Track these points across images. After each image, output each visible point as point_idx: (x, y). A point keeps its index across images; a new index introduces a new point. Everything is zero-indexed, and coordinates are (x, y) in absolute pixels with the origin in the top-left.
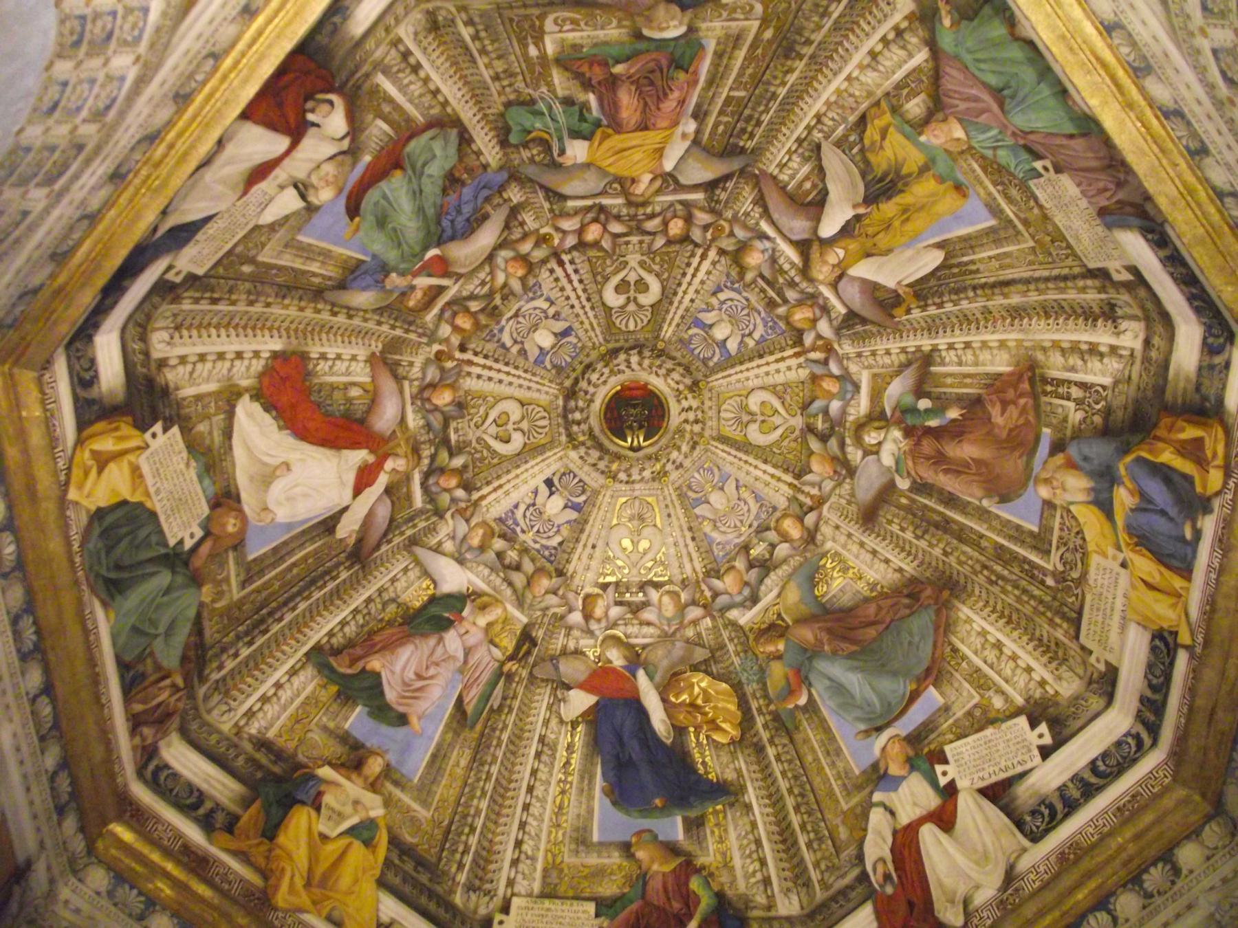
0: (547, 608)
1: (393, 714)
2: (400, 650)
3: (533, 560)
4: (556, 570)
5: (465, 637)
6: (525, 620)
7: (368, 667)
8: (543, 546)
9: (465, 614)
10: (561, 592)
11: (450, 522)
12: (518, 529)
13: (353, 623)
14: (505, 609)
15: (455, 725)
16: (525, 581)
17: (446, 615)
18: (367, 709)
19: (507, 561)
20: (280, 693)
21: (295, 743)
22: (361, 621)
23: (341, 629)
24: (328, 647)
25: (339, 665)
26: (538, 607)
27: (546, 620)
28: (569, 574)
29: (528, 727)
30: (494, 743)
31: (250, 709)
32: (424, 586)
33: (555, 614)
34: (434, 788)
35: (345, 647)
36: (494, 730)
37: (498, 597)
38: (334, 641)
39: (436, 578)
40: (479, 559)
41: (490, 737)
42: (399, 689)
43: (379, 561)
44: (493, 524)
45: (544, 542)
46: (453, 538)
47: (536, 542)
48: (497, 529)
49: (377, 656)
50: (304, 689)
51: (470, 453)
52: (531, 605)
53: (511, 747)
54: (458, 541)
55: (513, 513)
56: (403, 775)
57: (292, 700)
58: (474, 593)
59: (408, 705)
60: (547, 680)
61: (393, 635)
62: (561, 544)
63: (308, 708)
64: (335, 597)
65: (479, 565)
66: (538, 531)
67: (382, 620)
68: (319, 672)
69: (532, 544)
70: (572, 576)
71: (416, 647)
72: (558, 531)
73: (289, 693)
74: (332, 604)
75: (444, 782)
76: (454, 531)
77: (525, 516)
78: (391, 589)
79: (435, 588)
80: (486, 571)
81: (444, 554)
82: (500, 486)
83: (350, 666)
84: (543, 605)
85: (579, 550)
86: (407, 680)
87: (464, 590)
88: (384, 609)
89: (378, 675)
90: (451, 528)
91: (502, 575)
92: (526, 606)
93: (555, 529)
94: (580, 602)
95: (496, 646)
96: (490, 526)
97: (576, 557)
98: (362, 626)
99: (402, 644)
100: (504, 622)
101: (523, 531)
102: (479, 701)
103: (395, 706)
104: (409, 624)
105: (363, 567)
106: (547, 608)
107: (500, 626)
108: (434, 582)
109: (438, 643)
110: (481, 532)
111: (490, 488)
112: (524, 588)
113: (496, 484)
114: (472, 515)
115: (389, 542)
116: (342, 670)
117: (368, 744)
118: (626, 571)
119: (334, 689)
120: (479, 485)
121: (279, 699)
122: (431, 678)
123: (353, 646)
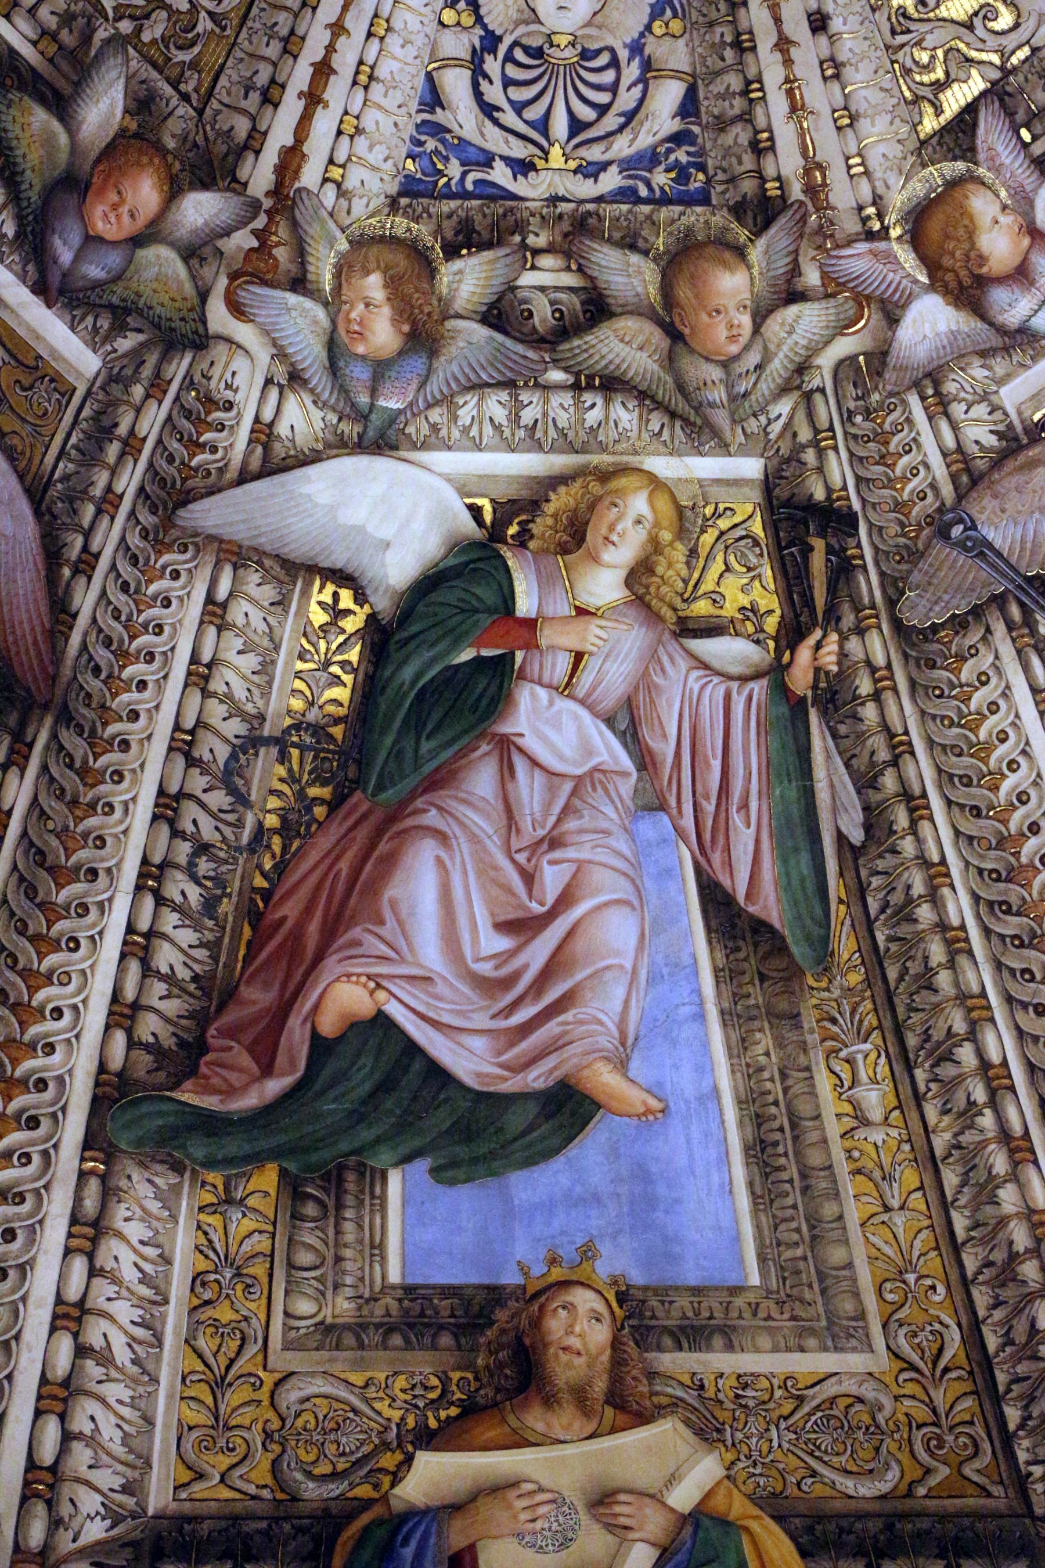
0: (802, 369)
1: (532, 1109)
2: (391, 892)
3: (630, 243)
4: (738, 211)
5: (585, 680)
6: (752, 467)
7: (328, 1025)
8: (627, 165)
9: (525, 605)
10: (812, 277)
11: (244, 332)
12: (500, 175)
13: (170, 920)
14: (655, 483)
15: (757, 996)
16: (657, 337)
17: (466, 655)
18: (421, 1166)
19: (543, 314)
20: (94, 1333)
21: (262, 1461)
22: (194, 894)
23: (148, 970)
24: (144, 1060)
25: (230, 1092)
26: (765, 387)
27: (825, 410)
28: (796, 192)
29: (1017, 820)
30: (937, 952)
31: (32, 1465)
32: (319, 617)
33: (845, 365)
34: (837, 1255)
35: (201, 1019)
36: (905, 913)
37: (596, 459)
38: (149, 1026)
39: (338, 559)
40: (436, 386)
41: (910, 945)
42: (481, 1020)
43: (102, 655)
44: (400, 225)
45: (622, 147)
46: (296, 378)
47: (593, 171)
48: (423, 231)
49: (331, 966)
50: (166, 1260)
51: (115, 41)
52: (733, 398)
53: (1011, 926)
54: (319, 378)
55: (438, 130)
56: (697, 1291)
57: (153, 1327)
58: (506, 510)
59: (554, 1046)
60: (977, 612)
61: (334, 855)
62: (689, 107)
63: (224, 1313)
64: (45, 881)
65: (448, 401)
66: (576, 126)
67: (260, 829)
68: (178, 1168)
69: (586, 189)
70: (811, 190)
71: (442, 837)
72: (647, 65)
73: (124, 1311)
74: (52, 912)
75: (853, 1214)
76: (280, 354)
77: (488, 110)
78: (216, 710)
79: (360, 598)
80: (496, 406)
81: (311, 459)
82: (323, 70)
83: (267, 1070)
84: (778, 367)
85: (773, 75)
86: (485, 969)
87: (467, 525)
88: (241, 799)
89: (381, 1021)
90: (263, 355)
91: (556, 376)
92: (721, 418)
93: (632, 71)
94: (906, 257)
95: (712, 629)
96: (392, 241)
97: (778, 104)
98: (210, 905)
99: (390, 862)
100: (681, 532)
101: (523, 167)
102: (784, 858)
103: (511, 1085)
104: (358, 783)
105: (66, 717)
106: (802, 369)
107: (679, 553)
108: (342, 577)
109: (508, 770)
110: (374, 285)
111: (291, 108)
112: (670, 361)
113: (301, 76)
114: (301, 253)
115: (86, 564)
116: (250, 1101)
117: (511, 1278)
118: (1005, 19)
119: (267, 1179)
120: (242, 126)
121: (105, 1358)
122: (565, 900)
123: (229, 995)
